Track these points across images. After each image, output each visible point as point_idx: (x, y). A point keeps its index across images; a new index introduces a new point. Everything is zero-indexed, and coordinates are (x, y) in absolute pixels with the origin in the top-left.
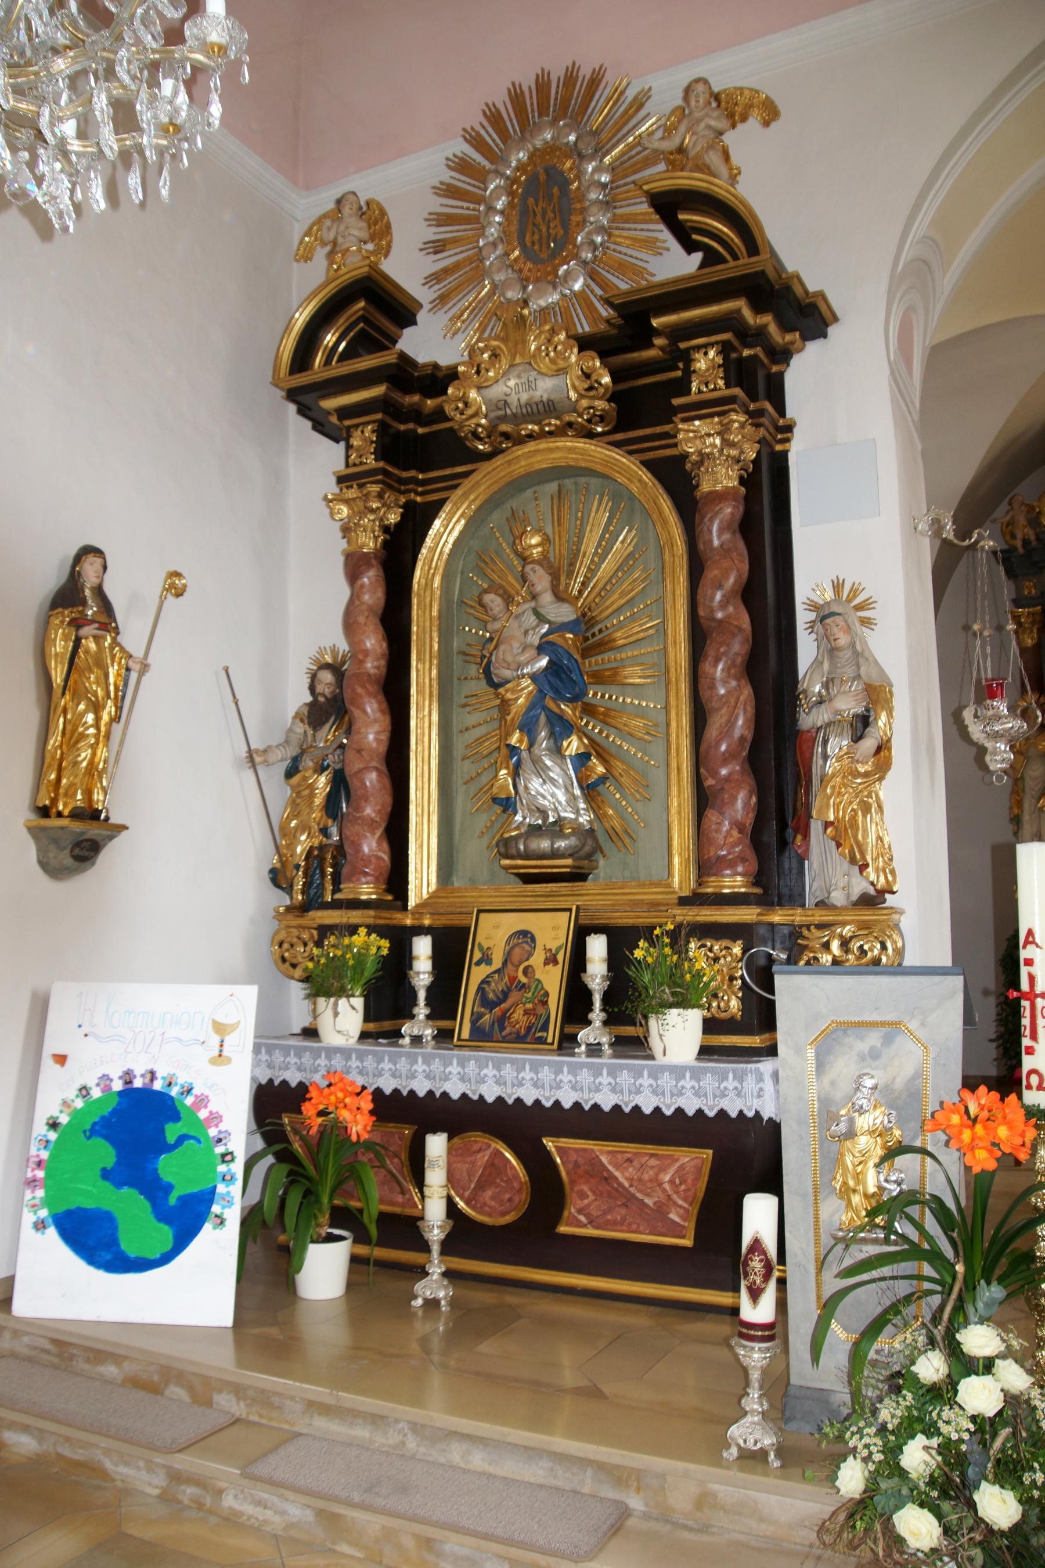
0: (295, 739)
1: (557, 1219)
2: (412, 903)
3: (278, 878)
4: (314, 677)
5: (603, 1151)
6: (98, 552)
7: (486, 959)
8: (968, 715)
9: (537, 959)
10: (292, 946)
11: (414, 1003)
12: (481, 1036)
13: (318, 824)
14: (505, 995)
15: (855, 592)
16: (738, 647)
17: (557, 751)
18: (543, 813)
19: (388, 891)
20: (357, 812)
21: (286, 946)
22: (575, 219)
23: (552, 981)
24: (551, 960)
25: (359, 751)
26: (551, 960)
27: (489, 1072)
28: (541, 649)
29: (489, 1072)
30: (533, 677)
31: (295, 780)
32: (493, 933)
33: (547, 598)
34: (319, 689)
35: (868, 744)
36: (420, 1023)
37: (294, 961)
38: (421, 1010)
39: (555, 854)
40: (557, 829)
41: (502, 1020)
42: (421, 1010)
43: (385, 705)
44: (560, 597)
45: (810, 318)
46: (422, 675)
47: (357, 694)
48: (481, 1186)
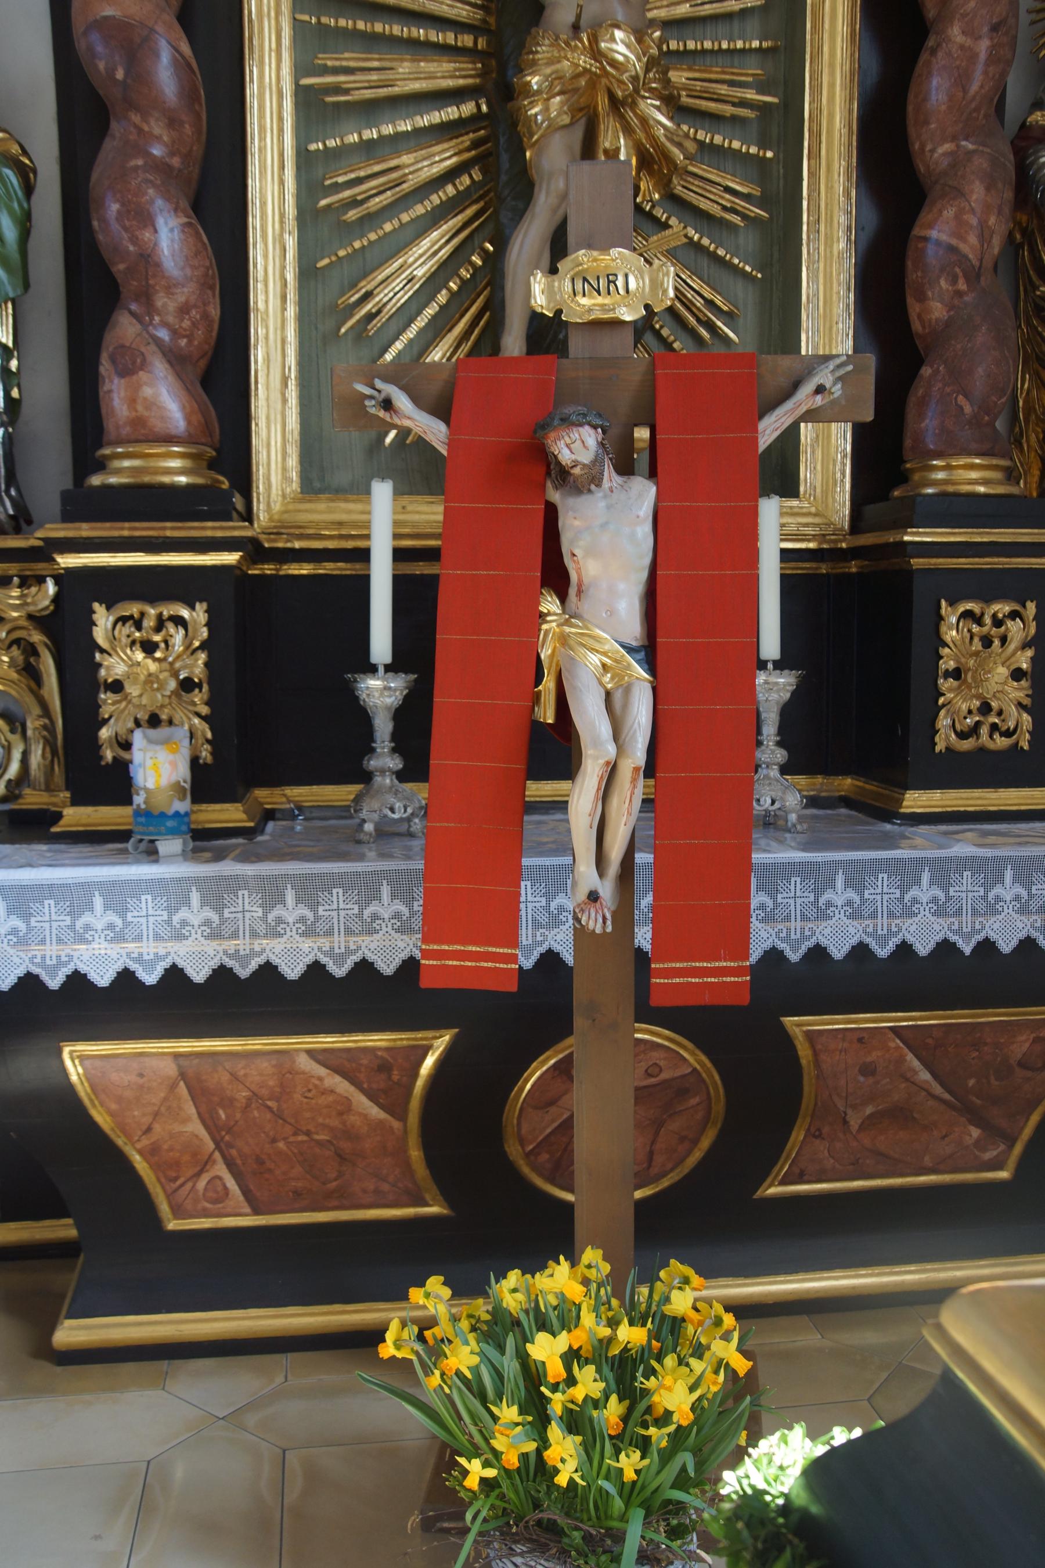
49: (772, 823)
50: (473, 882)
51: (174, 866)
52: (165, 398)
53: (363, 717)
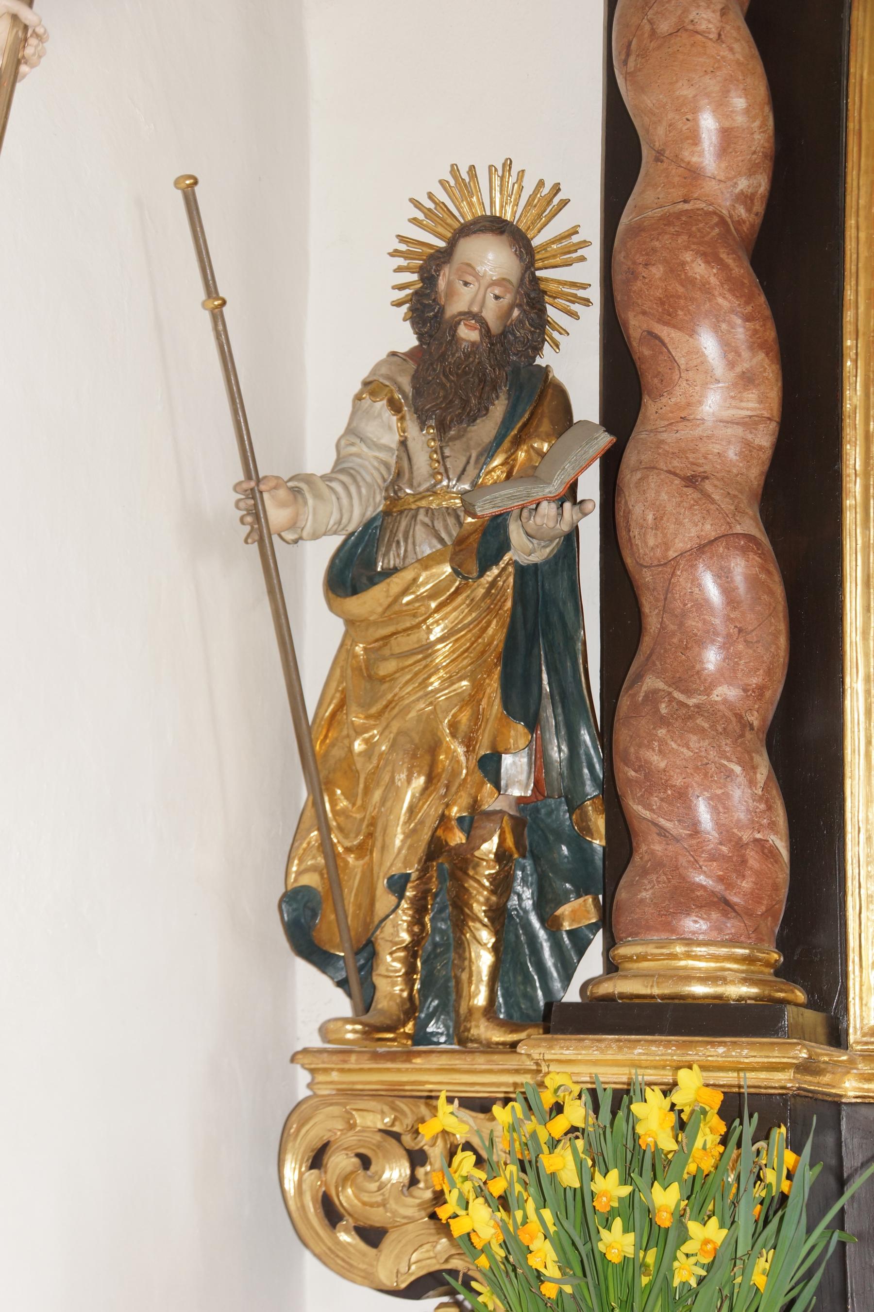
0: (373, 463)
4: (431, 266)
10: (365, 1162)
13: (469, 744)
19: (786, 972)
20: (688, 692)
21: (340, 1162)
25: (692, 481)
31: (370, 602)
37: (377, 1217)
43: (771, 334)
47: (689, 282)
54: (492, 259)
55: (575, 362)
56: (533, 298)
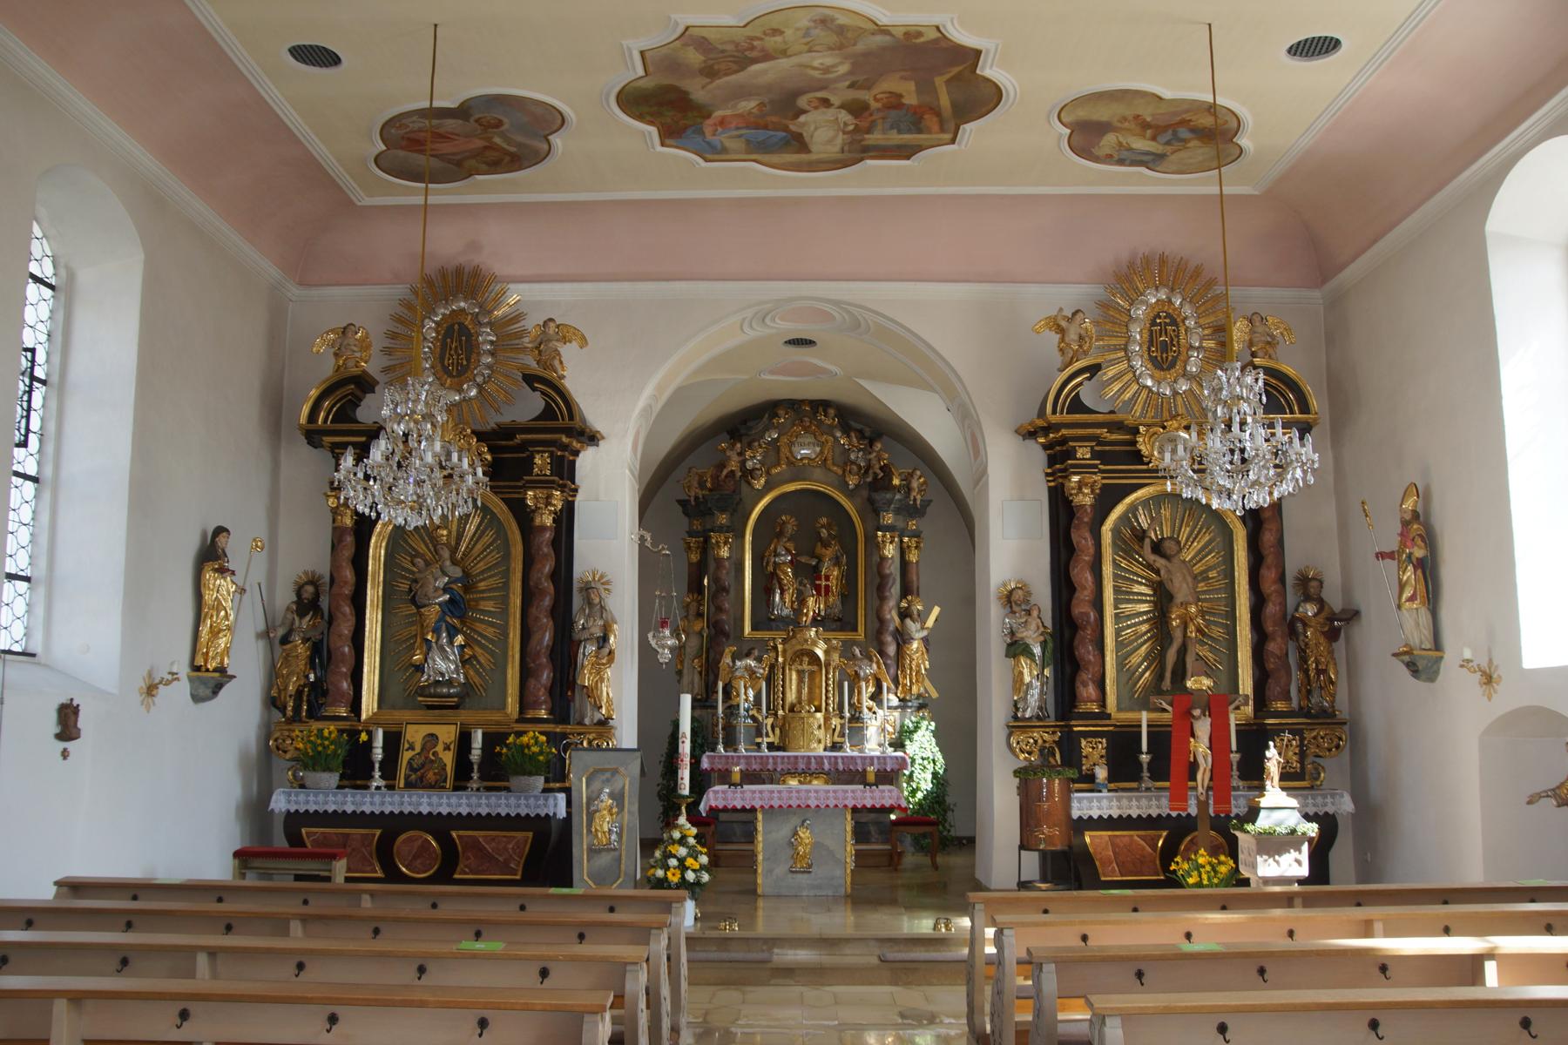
1: (454, 872)
2: (364, 716)
3: (273, 702)
5: (478, 834)
6: (227, 531)
7: (412, 748)
8: (650, 635)
9: (439, 748)
11: (373, 769)
12: (409, 785)
14: (423, 765)
15: (602, 577)
16: (547, 602)
17: (451, 642)
18: (442, 675)
22: (474, 356)
23: (448, 758)
24: (447, 748)
26: (447, 748)
27: (425, 800)
28: (445, 590)
29: (425, 800)
30: (440, 604)
32: (415, 734)
33: (448, 563)
34: (305, 595)
35: (606, 651)
36: (377, 781)
38: (377, 774)
39: (449, 696)
40: (450, 683)
41: (422, 778)
42: (377, 774)
44: (454, 562)
45: (593, 438)
46: (373, 594)
48: (415, 857)
49: (1237, 789)
50: (1179, 797)
51: (1105, 794)
52: (1091, 691)
53: (1141, 764)
54: (310, 589)
55: (324, 602)
56: (317, 595)
